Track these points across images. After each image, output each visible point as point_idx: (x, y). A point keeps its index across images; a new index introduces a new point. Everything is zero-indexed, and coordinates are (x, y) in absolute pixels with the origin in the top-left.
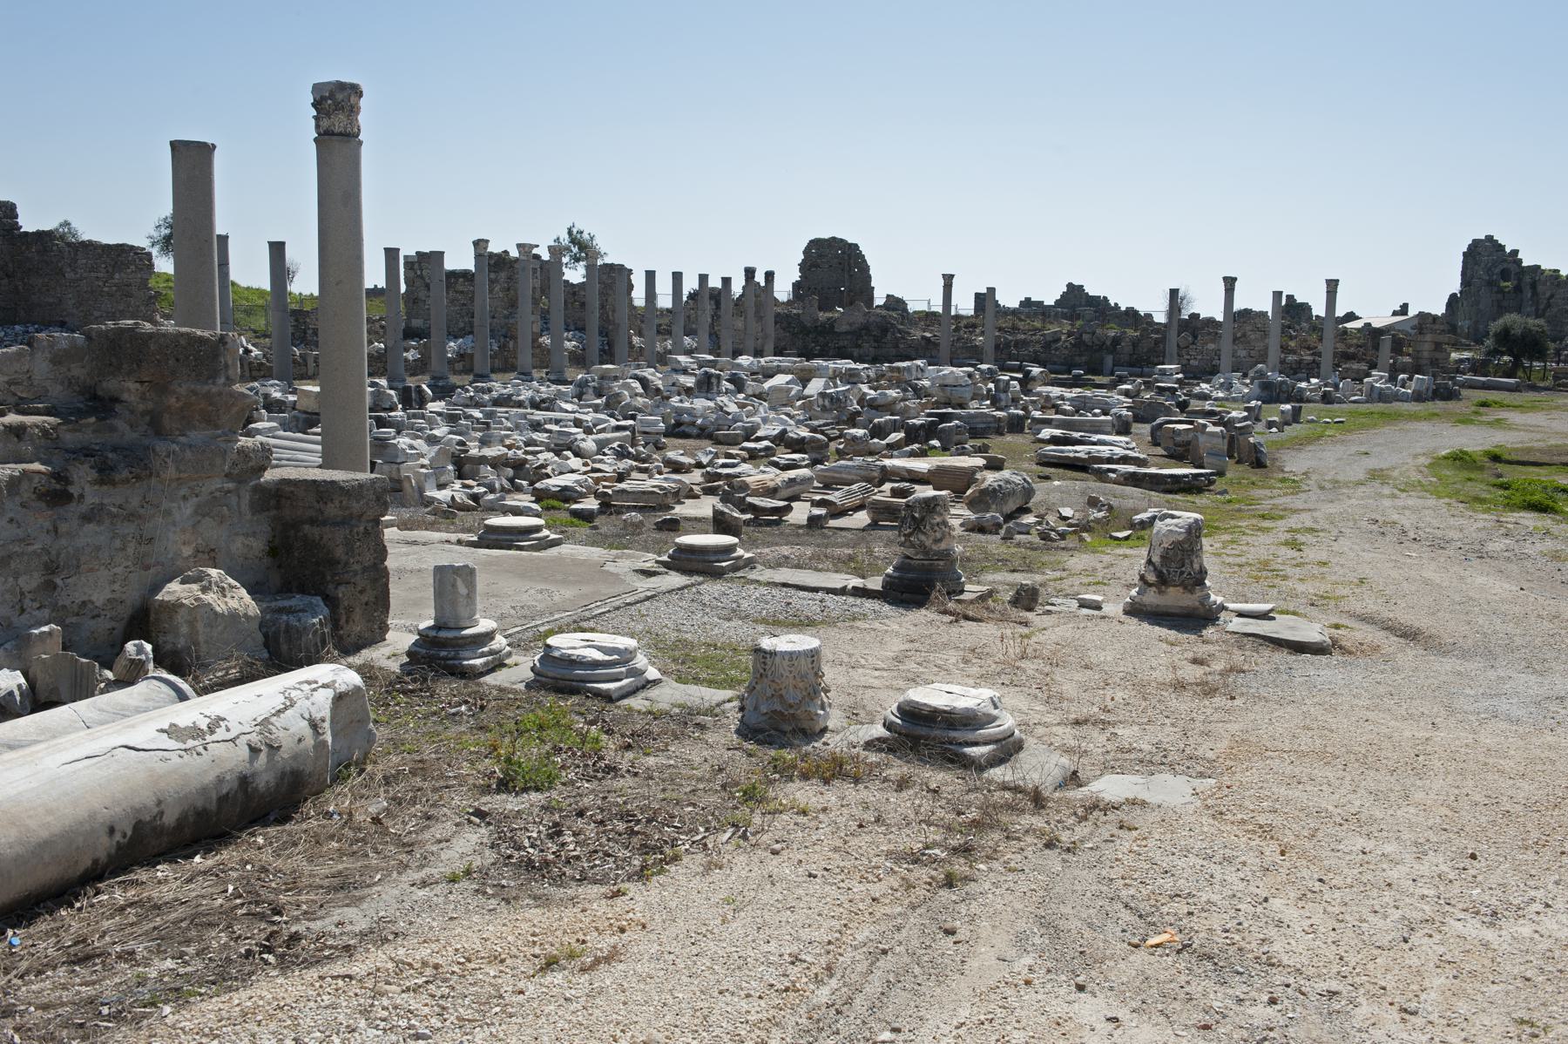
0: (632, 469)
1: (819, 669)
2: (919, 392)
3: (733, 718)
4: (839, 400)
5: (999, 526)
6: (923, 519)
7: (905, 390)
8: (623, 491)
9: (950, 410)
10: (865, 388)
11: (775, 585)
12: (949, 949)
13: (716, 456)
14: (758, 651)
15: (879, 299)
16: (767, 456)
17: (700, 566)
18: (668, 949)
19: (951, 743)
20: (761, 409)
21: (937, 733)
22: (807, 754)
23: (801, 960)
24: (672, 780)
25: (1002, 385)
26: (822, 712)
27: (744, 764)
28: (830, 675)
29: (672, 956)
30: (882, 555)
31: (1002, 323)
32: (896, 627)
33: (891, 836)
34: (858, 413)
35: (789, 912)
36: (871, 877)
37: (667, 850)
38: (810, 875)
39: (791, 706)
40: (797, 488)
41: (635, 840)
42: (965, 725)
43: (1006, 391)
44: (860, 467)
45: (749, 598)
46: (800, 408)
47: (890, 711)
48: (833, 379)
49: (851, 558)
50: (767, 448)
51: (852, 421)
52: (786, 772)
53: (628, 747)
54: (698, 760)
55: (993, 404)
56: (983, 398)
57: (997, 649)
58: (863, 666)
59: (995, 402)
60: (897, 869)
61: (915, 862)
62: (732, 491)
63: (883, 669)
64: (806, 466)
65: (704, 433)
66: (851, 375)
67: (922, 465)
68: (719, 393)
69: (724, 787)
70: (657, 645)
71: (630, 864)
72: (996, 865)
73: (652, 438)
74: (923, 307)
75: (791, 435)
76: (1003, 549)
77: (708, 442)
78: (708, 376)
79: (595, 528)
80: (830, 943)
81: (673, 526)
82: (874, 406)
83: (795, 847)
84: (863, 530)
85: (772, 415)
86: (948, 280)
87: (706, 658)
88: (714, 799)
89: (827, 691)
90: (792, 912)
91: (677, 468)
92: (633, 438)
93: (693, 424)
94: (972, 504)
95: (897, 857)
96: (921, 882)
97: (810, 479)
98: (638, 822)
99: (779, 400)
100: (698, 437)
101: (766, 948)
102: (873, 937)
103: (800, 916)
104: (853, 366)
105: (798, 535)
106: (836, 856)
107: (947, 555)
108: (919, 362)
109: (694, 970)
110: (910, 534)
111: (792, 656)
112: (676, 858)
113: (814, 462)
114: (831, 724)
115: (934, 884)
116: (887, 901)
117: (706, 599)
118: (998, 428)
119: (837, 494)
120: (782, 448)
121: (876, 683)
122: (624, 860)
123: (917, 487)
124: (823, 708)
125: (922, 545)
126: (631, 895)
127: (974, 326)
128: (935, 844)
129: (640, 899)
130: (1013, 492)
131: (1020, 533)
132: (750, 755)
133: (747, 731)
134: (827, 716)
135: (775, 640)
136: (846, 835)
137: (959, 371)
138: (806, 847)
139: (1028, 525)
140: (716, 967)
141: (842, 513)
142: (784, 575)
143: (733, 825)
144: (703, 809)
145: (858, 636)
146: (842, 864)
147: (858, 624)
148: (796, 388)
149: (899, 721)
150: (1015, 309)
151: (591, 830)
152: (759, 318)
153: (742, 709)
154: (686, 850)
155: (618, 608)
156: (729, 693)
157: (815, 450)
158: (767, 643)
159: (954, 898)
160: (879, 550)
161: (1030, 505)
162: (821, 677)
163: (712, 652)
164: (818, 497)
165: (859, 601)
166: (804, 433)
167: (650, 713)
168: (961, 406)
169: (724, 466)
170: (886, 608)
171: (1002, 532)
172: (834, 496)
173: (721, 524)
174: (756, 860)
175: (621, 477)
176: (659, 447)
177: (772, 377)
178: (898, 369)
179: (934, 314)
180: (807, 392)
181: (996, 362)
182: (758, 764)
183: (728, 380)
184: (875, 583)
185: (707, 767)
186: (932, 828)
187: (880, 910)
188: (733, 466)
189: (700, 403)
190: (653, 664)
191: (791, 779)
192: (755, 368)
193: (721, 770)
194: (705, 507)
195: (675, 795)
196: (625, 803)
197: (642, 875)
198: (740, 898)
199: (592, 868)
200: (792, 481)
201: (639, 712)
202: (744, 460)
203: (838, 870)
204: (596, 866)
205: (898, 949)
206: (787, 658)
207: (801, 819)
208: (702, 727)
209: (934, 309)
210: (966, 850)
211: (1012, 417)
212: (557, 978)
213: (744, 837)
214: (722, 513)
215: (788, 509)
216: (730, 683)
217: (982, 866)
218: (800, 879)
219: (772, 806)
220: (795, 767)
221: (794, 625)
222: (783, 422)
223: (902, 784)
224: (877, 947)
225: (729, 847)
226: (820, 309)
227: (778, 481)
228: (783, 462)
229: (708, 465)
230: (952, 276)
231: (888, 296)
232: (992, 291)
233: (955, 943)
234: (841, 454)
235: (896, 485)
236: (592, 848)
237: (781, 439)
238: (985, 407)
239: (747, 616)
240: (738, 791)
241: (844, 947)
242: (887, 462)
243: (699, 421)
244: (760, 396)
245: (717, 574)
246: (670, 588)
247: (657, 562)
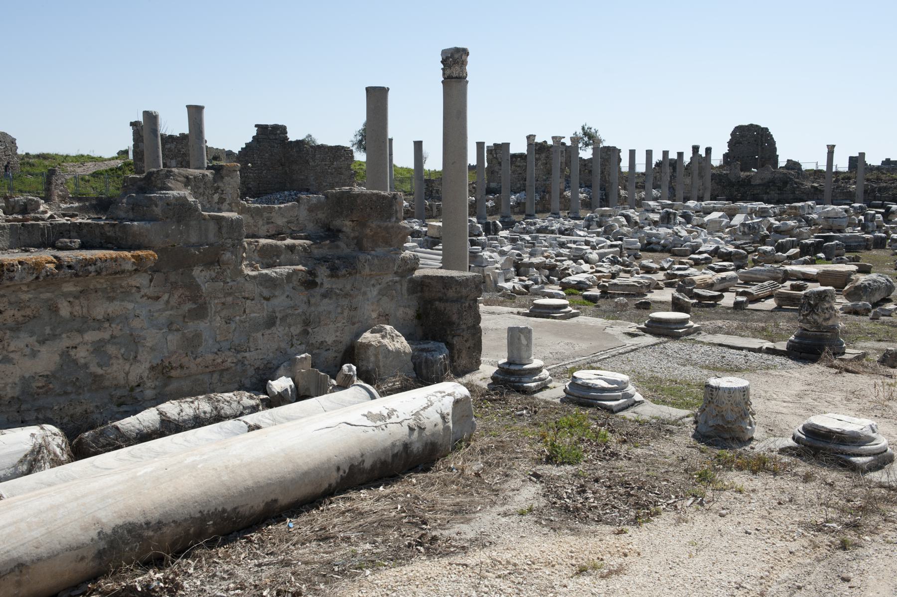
0: (620, 271)
1: (748, 400)
2: (809, 222)
3: (691, 429)
4: (754, 228)
5: (869, 311)
6: (816, 305)
7: (800, 221)
8: (615, 284)
9: (832, 234)
10: (772, 220)
11: (714, 345)
12: (846, 591)
13: (674, 263)
14: (708, 386)
15: (782, 162)
16: (706, 263)
17: (665, 331)
18: (655, 570)
19: (842, 454)
20: (703, 234)
21: (832, 446)
22: (740, 454)
23: (743, 587)
24: (653, 464)
25: (869, 217)
26: (750, 428)
27: (700, 457)
28: (756, 404)
29: (657, 575)
30: (785, 328)
31: (869, 176)
32: (797, 375)
33: (802, 512)
34: (767, 236)
35: (733, 555)
36: (788, 538)
37: (651, 507)
38: (746, 532)
39: (728, 422)
40: (726, 284)
41: (631, 500)
42: (853, 442)
43: (872, 221)
44: (769, 271)
45: (698, 352)
46: (728, 233)
47: (797, 428)
48: (750, 214)
49: (764, 329)
50: (706, 259)
51: (763, 241)
52: (728, 465)
53: (624, 442)
54: (668, 453)
55: (863, 230)
56: (855, 226)
57: (870, 392)
58: (775, 399)
59: (864, 228)
60: (806, 534)
61: (819, 530)
62: (684, 285)
63: (789, 402)
64: (732, 270)
65: (666, 249)
66: (762, 212)
67: (812, 270)
68: (675, 224)
69: (686, 471)
70: (639, 379)
71: (628, 514)
72: (877, 538)
73: (633, 252)
74: (813, 167)
75: (722, 250)
76: (871, 326)
77: (667, 255)
78: (668, 213)
79: (598, 306)
80: (762, 578)
81: (646, 306)
82: (778, 231)
83: (735, 513)
84: (772, 311)
85: (709, 237)
86: (831, 150)
87: (670, 389)
88: (679, 478)
89: (753, 414)
90: (735, 555)
91: (648, 270)
92: (621, 252)
93: (658, 243)
94: (848, 296)
95: (808, 526)
96: (823, 544)
97: (735, 278)
98: (632, 488)
99: (714, 228)
100: (662, 251)
101: (719, 576)
102: (791, 577)
103: (740, 558)
104: (764, 206)
105: (727, 313)
106: (764, 521)
107: (833, 329)
108: (810, 203)
109: (672, 585)
110: (807, 315)
111: (730, 390)
112: (657, 513)
113: (738, 268)
114: (756, 435)
115: (833, 546)
116: (800, 555)
117: (670, 352)
118: (866, 245)
119: (753, 287)
120: (715, 259)
121: (784, 410)
122: (624, 511)
123: (809, 284)
124: (750, 425)
125: (815, 322)
126: (630, 533)
127: (849, 178)
128: (832, 520)
129: (636, 536)
130: (879, 288)
131: (883, 315)
132: (702, 452)
133: (700, 436)
134: (753, 431)
135: (718, 380)
136: (770, 509)
137: (839, 208)
138: (743, 514)
139: (890, 310)
140: (686, 585)
141: (757, 300)
142: (720, 338)
143: (694, 496)
144: (673, 484)
145: (771, 379)
146: (768, 527)
147: (771, 371)
148: (726, 221)
149: (804, 437)
150: (879, 166)
151: (603, 491)
152: (701, 176)
153: (696, 422)
154: (664, 509)
155: (614, 356)
156: (686, 412)
157: (739, 260)
158: (713, 382)
159: (848, 557)
160: (783, 324)
161: (891, 297)
162: (749, 405)
163: (674, 385)
164: (741, 290)
165: (771, 357)
166: (731, 249)
167: (637, 421)
168: (840, 231)
169: (679, 269)
170: (790, 362)
171: (871, 315)
172: (752, 289)
173: (677, 305)
174: (710, 519)
175: (614, 276)
176: (637, 258)
177: (710, 213)
178: (795, 208)
179: (821, 171)
180: (733, 223)
181: (864, 202)
182: (707, 458)
183: (680, 216)
184: (782, 346)
185: (674, 457)
186: (830, 509)
187: (795, 560)
188: (685, 269)
189: (663, 231)
190: (637, 391)
191: (730, 469)
192: (698, 208)
193: (683, 460)
194: (667, 295)
195: (655, 474)
196: (623, 476)
197: (636, 522)
198: (700, 543)
199: (605, 514)
200: (723, 279)
201: (630, 420)
202: (691, 266)
203: (765, 531)
204: (607, 513)
205: (809, 587)
206: (727, 392)
207: (738, 495)
208: (671, 432)
209: (820, 168)
210: (855, 526)
211: (877, 238)
212: (586, 580)
213: (701, 504)
214: (678, 299)
215: (721, 297)
216: (687, 406)
217: (867, 538)
218: (740, 534)
219: (719, 486)
220: (733, 461)
221: (727, 371)
222: (717, 242)
223: (807, 478)
224: (794, 584)
225: (691, 509)
226: (742, 170)
227: (714, 279)
228: (717, 267)
229: (668, 269)
230: (834, 146)
231: (788, 161)
232: (862, 155)
233: (850, 587)
234: (755, 262)
235: (794, 282)
236: (604, 502)
237: (716, 253)
238: (857, 232)
239: (696, 364)
240: (696, 474)
241: (771, 581)
242: (788, 268)
243: (662, 242)
244: (702, 226)
245: (676, 337)
246: (646, 344)
247: (638, 328)
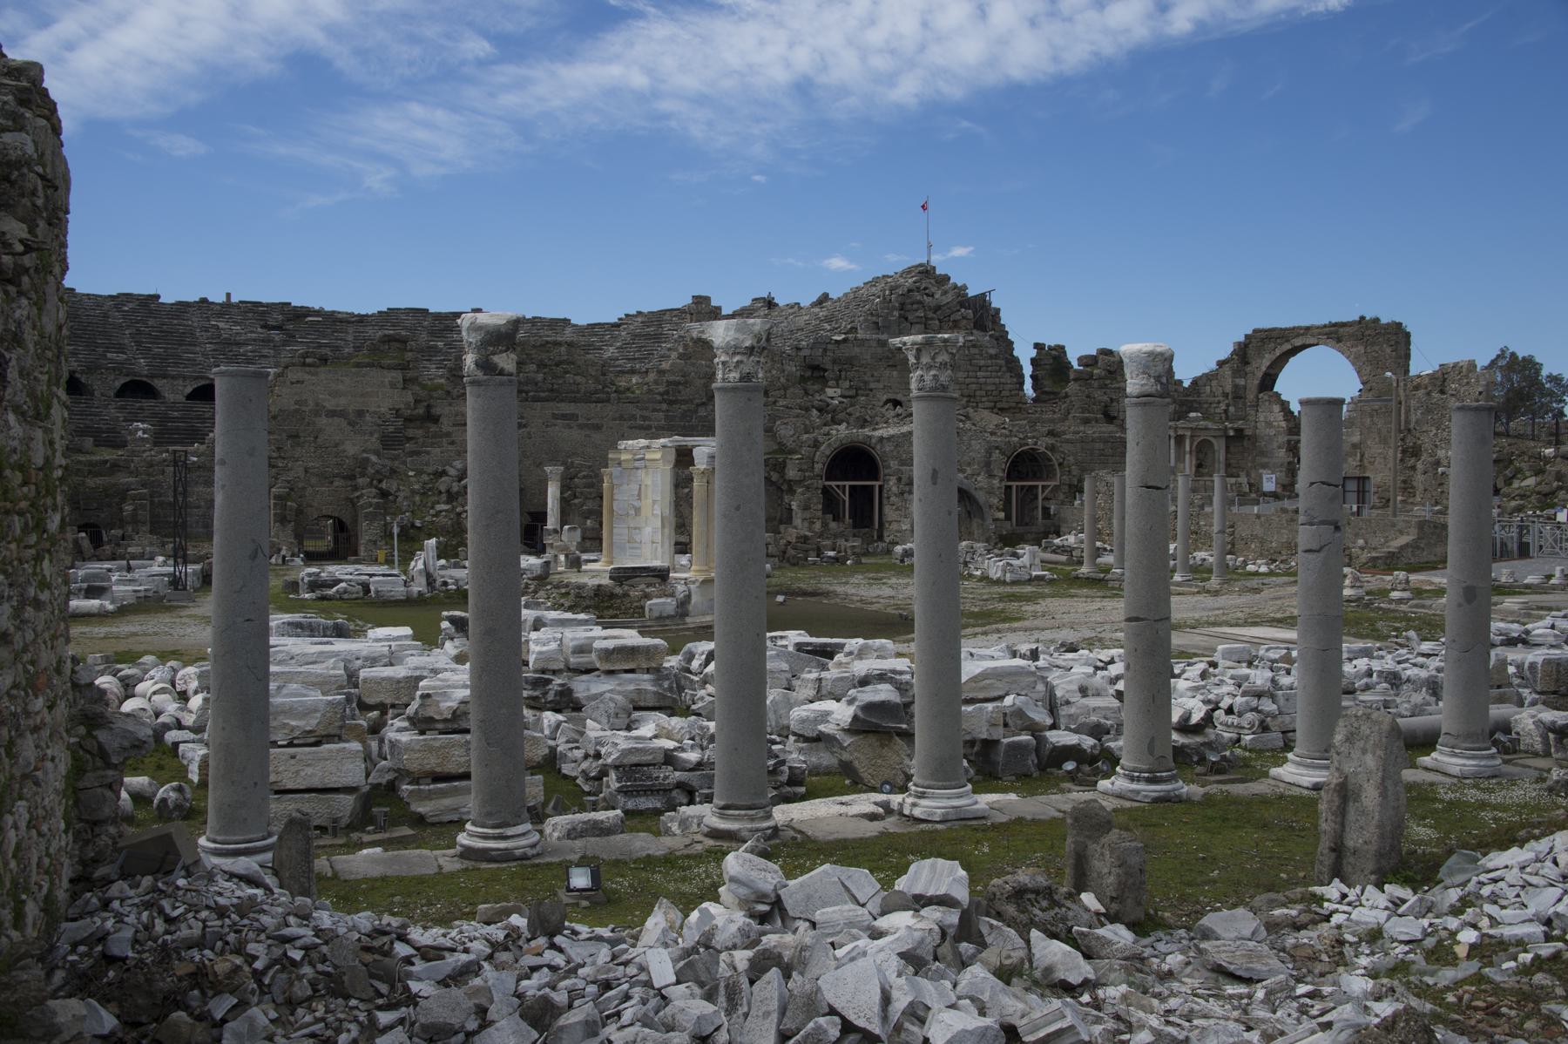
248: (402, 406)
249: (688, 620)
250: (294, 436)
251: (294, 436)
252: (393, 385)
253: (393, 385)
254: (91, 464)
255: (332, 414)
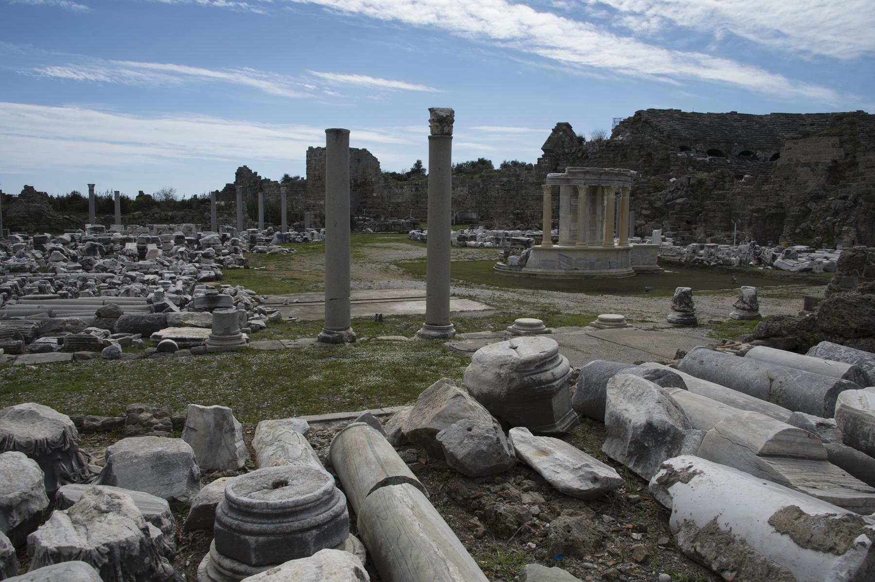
230: (93, 185)
248: (838, 158)
249: (524, 269)
250: (787, 179)
251: (787, 178)
252: (834, 146)
253: (834, 146)
254: (719, 195)
255: (804, 165)
